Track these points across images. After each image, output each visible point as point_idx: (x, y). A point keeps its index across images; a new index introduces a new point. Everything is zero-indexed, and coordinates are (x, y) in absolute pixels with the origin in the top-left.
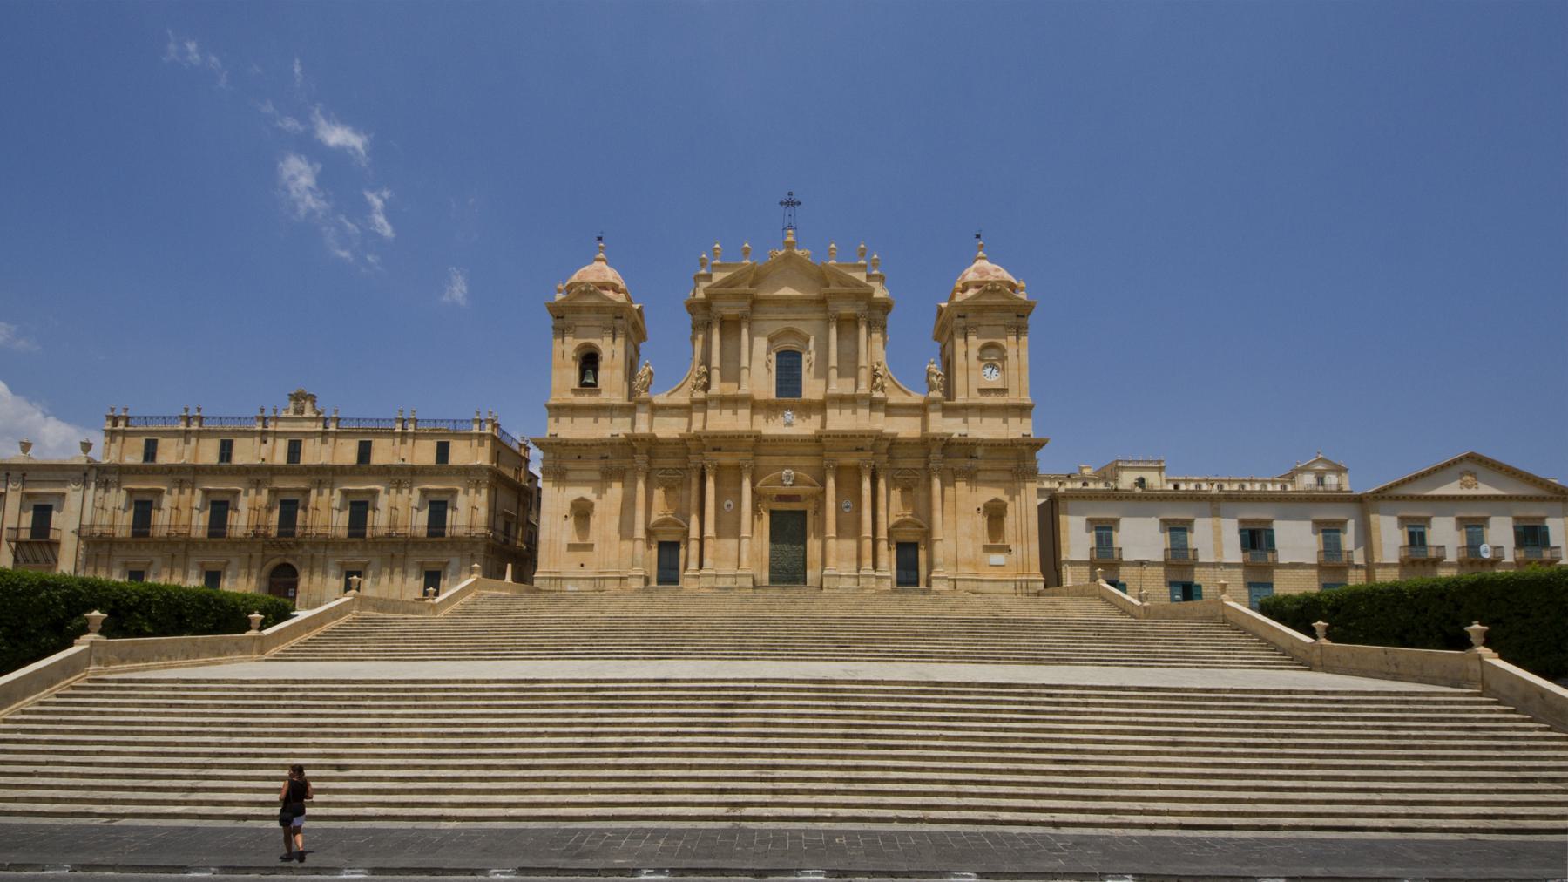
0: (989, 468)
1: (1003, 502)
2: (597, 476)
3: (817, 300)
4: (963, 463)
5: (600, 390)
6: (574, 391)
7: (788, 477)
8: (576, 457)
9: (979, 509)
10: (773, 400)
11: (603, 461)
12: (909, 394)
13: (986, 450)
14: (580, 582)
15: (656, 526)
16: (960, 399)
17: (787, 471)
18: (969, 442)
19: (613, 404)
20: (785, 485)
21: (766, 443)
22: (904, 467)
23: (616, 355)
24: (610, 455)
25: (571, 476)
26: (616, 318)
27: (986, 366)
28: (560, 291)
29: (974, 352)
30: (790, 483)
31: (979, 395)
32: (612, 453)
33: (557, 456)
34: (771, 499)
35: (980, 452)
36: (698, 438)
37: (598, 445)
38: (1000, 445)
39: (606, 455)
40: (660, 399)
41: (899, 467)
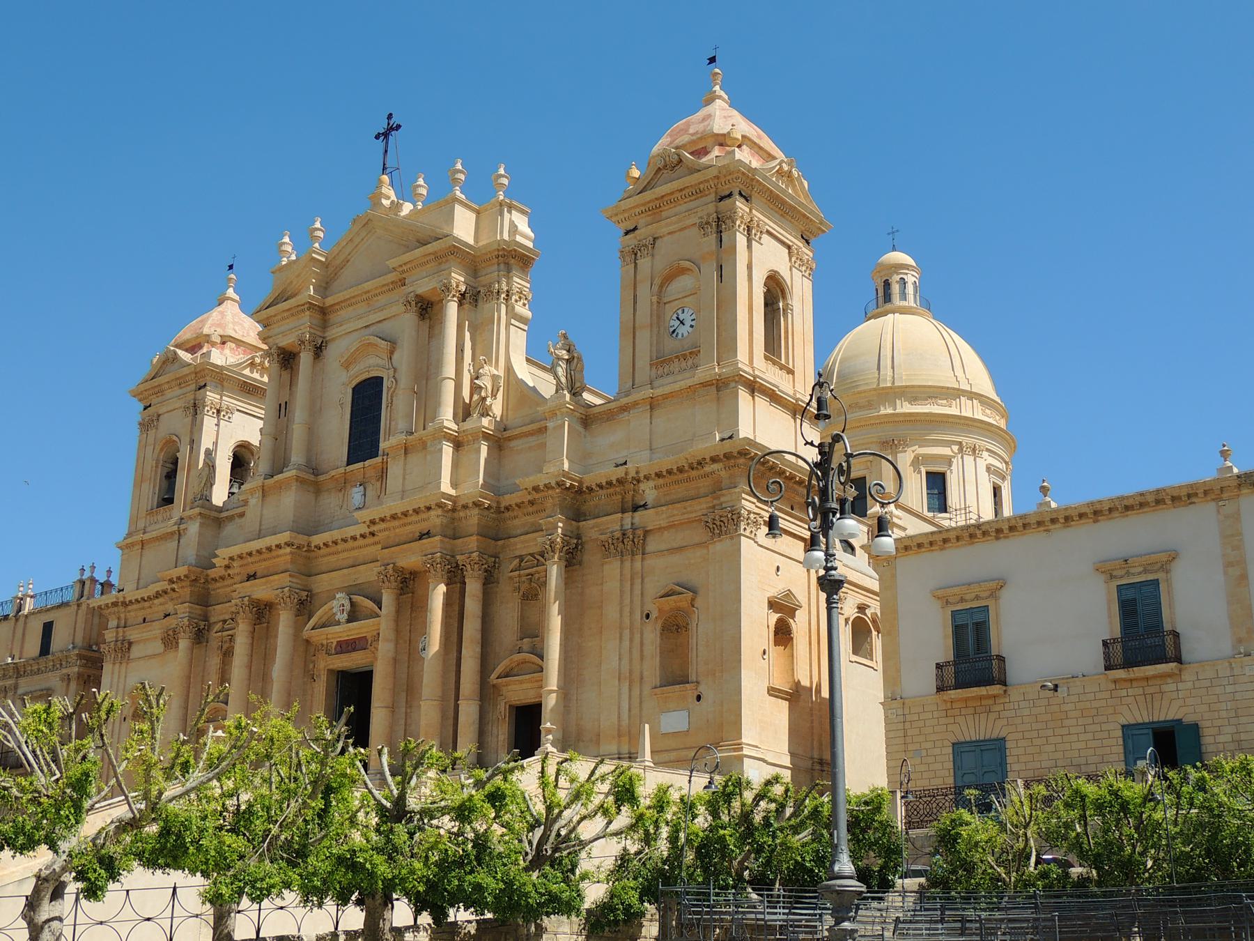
0: (664, 523)
2: (158, 647)
4: (614, 523)
9: (648, 616)
20: (338, 623)
25: (136, 651)
30: (345, 616)
35: (649, 492)
41: (518, 553)
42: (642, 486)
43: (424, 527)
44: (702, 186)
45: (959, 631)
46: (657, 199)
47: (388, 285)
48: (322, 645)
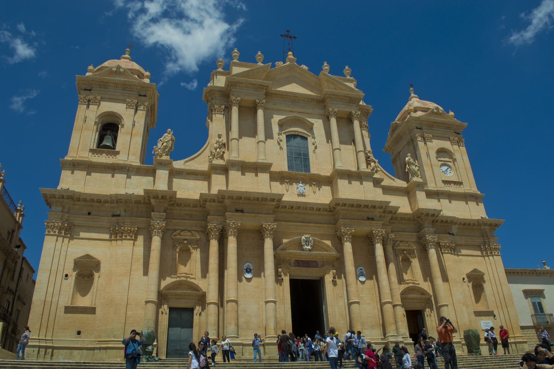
1: (480, 272)
3: (316, 100)
5: (118, 153)
6: (91, 151)
7: (307, 242)
8: (86, 212)
9: (464, 279)
10: (286, 172)
11: (115, 218)
12: (394, 180)
13: (459, 228)
14: (75, 352)
15: (169, 289)
16: (431, 186)
17: (306, 236)
18: (449, 220)
19: (131, 166)
20: (303, 250)
21: (283, 210)
22: (400, 239)
23: (136, 124)
24: (123, 213)
26: (140, 95)
27: (442, 165)
28: (90, 71)
29: (433, 154)
30: (309, 247)
31: (443, 184)
32: (125, 211)
33: (66, 210)
34: (290, 264)
35: (454, 229)
36: (222, 197)
37: (112, 202)
38: (469, 224)
39: (118, 213)
40: (178, 164)
42: (454, 226)
43: (370, 215)
44: (451, 126)
45: (534, 304)
46: (434, 122)
47: (309, 99)
48: (286, 260)
